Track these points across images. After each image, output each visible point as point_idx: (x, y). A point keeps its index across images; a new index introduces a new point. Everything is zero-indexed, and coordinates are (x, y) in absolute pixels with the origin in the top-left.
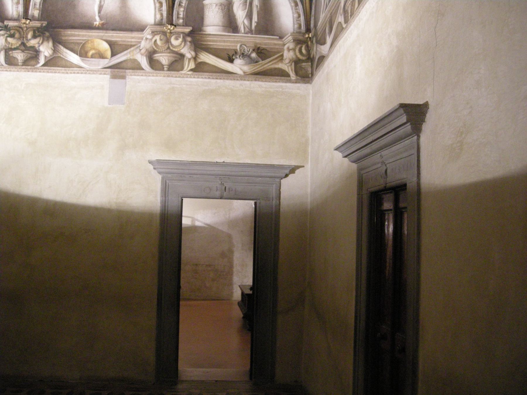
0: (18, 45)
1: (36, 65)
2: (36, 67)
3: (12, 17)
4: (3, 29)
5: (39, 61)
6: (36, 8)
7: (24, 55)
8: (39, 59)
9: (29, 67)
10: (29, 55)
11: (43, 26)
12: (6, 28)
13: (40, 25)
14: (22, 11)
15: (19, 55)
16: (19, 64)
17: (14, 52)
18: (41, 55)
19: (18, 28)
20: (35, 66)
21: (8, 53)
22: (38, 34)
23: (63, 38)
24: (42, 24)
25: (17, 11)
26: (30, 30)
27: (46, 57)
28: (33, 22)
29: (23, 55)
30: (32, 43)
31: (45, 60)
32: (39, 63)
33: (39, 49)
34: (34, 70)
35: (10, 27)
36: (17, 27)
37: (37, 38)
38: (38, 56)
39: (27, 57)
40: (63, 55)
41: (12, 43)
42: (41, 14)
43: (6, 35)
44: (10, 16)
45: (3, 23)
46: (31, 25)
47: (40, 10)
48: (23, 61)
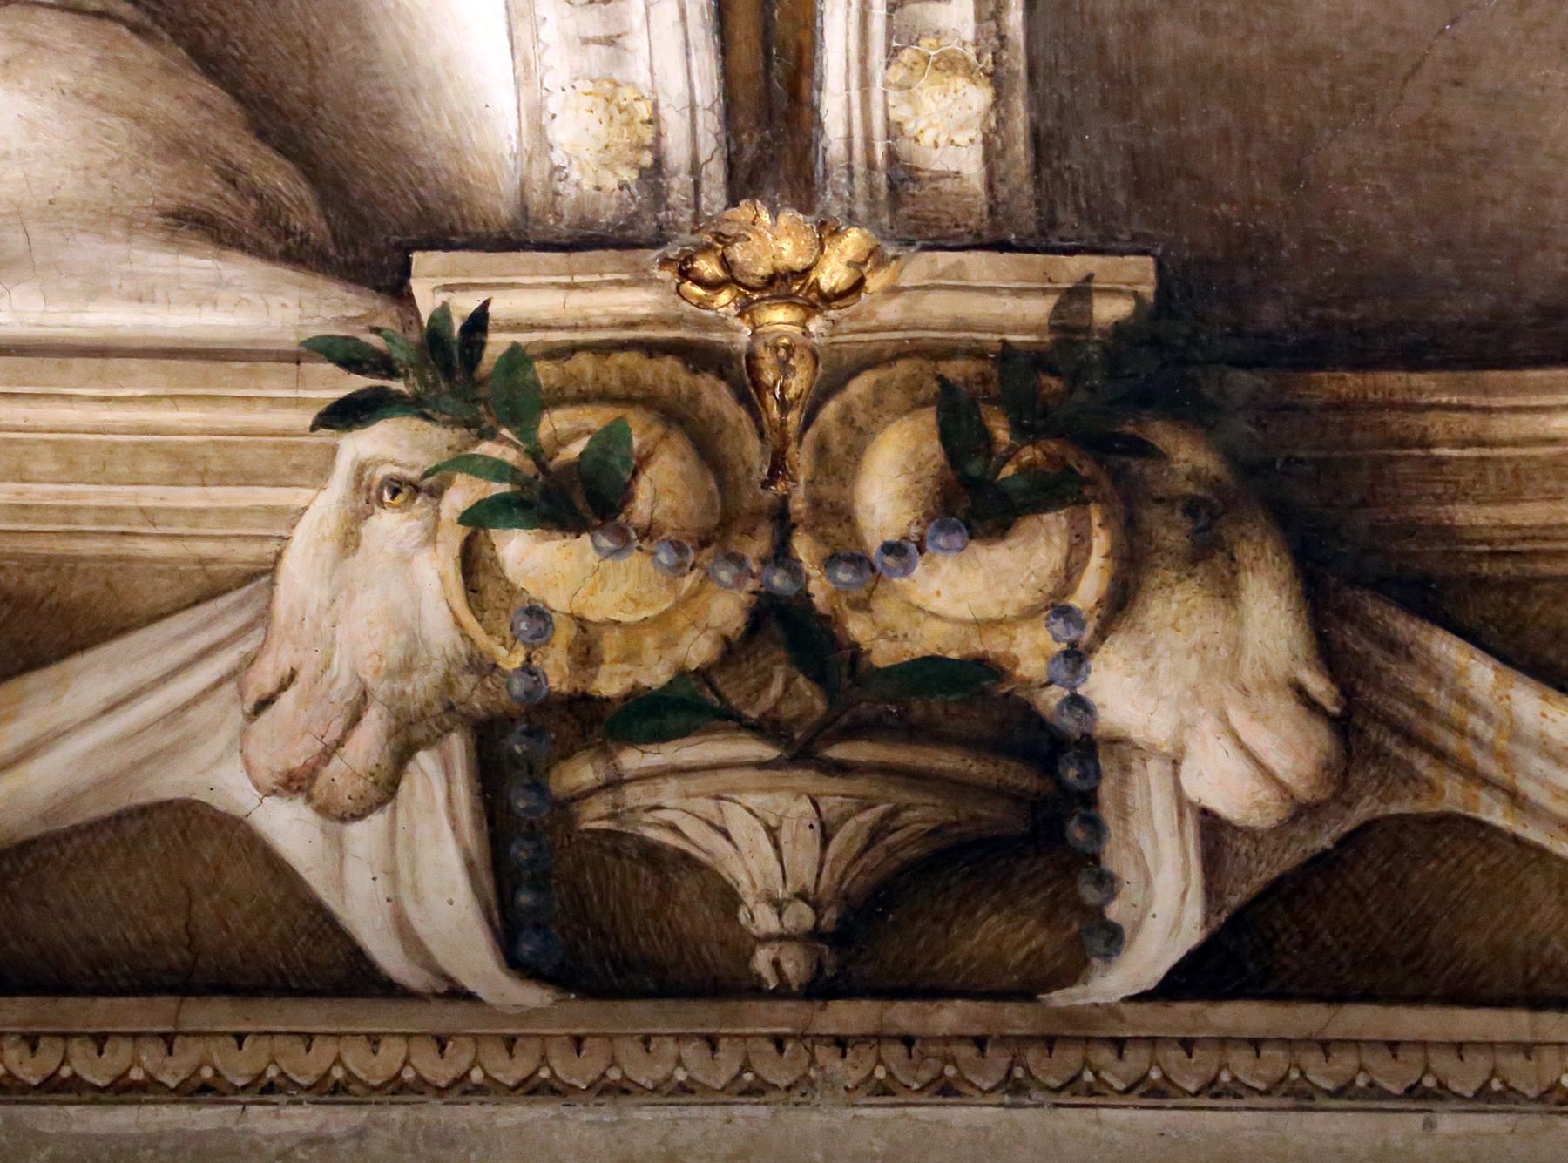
0: (698, 650)
1: (1073, 972)
2: (1068, 1015)
3: (536, 198)
4: (398, 385)
5: (1115, 911)
6: (926, 45)
7: (830, 804)
8: (1107, 883)
9: (948, 1016)
10: (922, 812)
11: (1088, 330)
12: (448, 371)
13: (1038, 309)
14: (707, 90)
15: (737, 820)
16: (762, 960)
17: (632, 760)
18: (1124, 814)
19: (669, 367)
20: (1058, 999)
21: (539, 788)
22: (1028, 454)
23: (1465, 514)
24: (1082, 292)
25: (610, 96)
26: (878, 397)
27: (1213, 829)
28: (921, 266)
29: (806, 806)
30: (936, 605)
31: (1212, 891)
32: (1114, 939)
33: (1077, 702)
34: (1052, 1068)
35: (516, 358)
36: (651, 349)
37: (1028, 524)
38: (1077, 833)
39: (876, 834)
40: (1515, 799)
41: (581, 622)
42: (1039, 141)
43: (462, 494)
44: (508, 186)
45: (398, 290)
46: (890, 311)
47: (998, 81)
48: (816, 906)
